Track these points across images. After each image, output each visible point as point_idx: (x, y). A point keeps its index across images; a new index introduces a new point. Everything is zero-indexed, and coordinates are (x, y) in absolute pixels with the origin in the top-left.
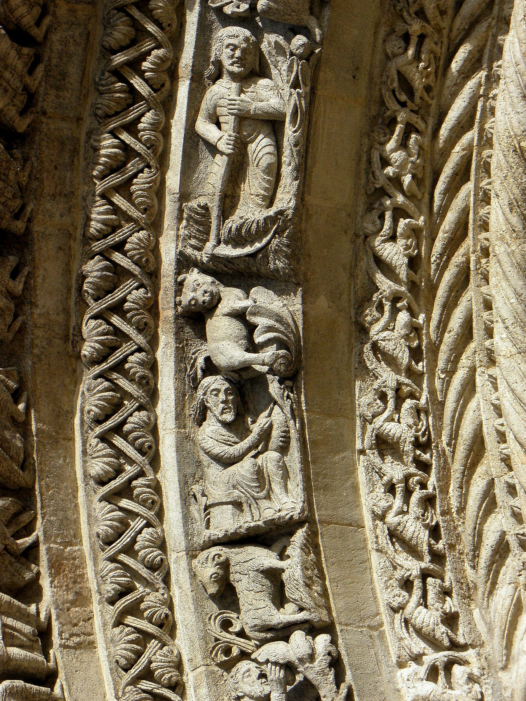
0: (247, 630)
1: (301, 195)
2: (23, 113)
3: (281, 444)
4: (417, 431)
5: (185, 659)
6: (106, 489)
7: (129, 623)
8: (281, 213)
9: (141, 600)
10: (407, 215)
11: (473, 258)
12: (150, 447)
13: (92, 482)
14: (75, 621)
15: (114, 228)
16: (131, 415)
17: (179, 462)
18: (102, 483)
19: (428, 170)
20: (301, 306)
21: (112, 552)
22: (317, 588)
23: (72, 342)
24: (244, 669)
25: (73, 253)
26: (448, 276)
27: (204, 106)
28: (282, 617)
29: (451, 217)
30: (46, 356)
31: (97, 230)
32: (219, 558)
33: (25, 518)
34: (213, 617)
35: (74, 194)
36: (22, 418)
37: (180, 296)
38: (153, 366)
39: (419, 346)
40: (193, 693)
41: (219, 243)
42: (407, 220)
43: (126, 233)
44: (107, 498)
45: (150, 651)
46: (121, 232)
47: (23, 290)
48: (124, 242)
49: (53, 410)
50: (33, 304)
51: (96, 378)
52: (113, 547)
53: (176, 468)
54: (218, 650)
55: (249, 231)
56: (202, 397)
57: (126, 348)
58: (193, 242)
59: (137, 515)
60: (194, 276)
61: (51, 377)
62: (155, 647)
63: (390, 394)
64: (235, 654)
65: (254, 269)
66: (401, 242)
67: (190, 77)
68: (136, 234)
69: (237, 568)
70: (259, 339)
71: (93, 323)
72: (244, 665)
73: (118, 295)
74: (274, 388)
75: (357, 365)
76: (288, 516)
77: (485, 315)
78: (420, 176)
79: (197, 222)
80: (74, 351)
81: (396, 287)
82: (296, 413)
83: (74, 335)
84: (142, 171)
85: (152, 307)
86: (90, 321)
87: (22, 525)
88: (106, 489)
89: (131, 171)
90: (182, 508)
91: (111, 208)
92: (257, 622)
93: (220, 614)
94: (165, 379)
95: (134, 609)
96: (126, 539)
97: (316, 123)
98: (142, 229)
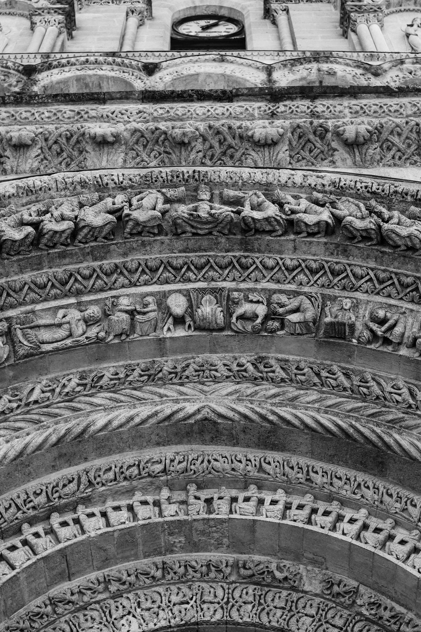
1: (47, 352)
2: (46, 245)
11: (45, 423)
15: (14, 291)
29: (57, 411)
41: (21, 329)
48: (11, 296)
58: (19, 321)
66: (42, 395)
77: (24, 434)
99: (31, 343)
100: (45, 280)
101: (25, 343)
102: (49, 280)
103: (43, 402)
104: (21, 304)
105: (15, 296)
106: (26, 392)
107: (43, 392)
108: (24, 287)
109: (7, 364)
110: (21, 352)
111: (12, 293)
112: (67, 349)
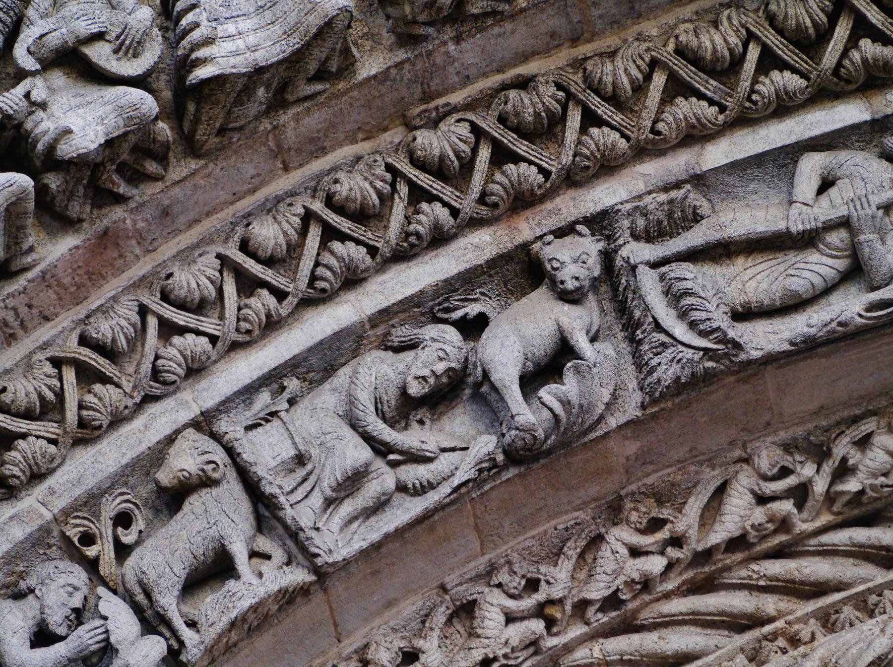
0: (131, 561)
1: (771, 360)
3: (410, 486)
4: (505, 656)
5: (51, 481)
6: (240, 258)
7: (65, 378)
8: (737, 346)
9: (105, 380)
10: (800, 506)
11: (780, 624)
12: (324, 290)
13: (240, 231)
14: (34, 302)
15: (614, 99)
16: (358, 242)
17: (321, 343)
18: (245, 246)
19: (878, 505)
20: (614, 426)
21: (154, 307)
22: (234, 636)
23: (425, 111)
24: (75, 582)
25: (553, 52)
26: (738, 602)
27: (842, 156)
28: (174, 607)
30: (391, 87)
31: (601, 79)
32: (214, 469)
33: (152, 167)
34: (126, 497)
35: (638, 18)
36: (290, 98)
37: (556, 237)
38: (439, 238)
39: (623, 602)
40: (7, 515)
41: (654, 265)
42: (795, 511)
43: (614, 120)
44: (224, 261)
45: (40, 428)
46: (613, 112)
47: (473, 15)
48: (600, 123)
49: (318, 131)
50: (458, 39)
51: (389, 168)
52: (162, 306)
53: (310, 343)
54: (84, 526)
55: (692, 308)
56: (427, 338)
57: (447, 192)
58: (641, 223)
59: (222, 317)
60: (589, 247)
61: (363, 106)
62: (47, 432)
63: (540, 596)
64: (88, 553)
65: (639, 334)
66: (759, 515)
67: (876, 117)
68: (618, 135)
69: (211, 504)
70: (547, 393)
71: (464, 130)
72: (79, 576)
73: (522, 147)
74: (486, 444)
75: (561, 527)
76: (316, 551)
78: (865, 499)
79: (670, 215)
80: (414, 118)
81: (693, 533)
82: (463, 490)
83: (437, 108)
84: (711, 102)
85: (523, 201)
86: (467, 124)
87: (139, 168)
88: (240, 258)
89: (706, 88)
90: (259, 379)
91: (641, 82)
92: (152, 575)
93: (135, 504)
94: (428, 268)
95: (88, 376)
96: (180, 318)
97: (884, 335)
98: (628, 139)
99: (703, 334)
100: (733, 40)
101: (680, 330)
102: (751, 36)
103: (763, 538)
104: (642, 151)
105: (619, 118)
106: (694, 506)
107: (762, 500)
108: (648, 78)
109: (613, 422)
110: (667, 371)
111: (603, 110)
112: (843, 338)
